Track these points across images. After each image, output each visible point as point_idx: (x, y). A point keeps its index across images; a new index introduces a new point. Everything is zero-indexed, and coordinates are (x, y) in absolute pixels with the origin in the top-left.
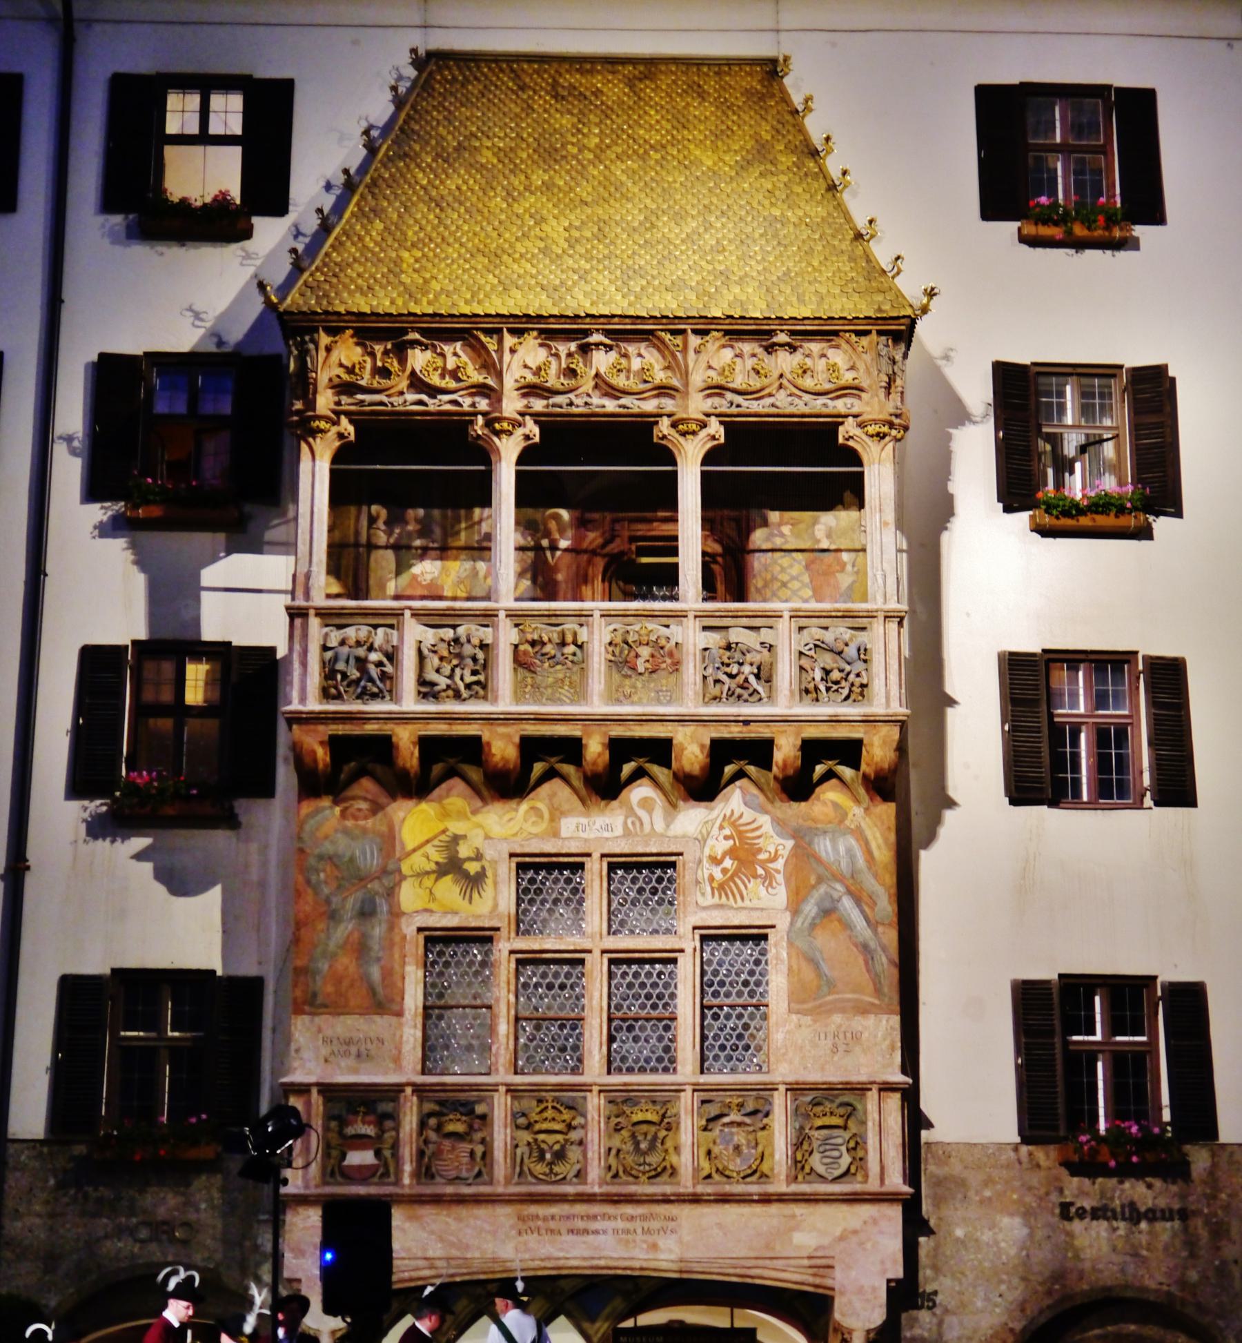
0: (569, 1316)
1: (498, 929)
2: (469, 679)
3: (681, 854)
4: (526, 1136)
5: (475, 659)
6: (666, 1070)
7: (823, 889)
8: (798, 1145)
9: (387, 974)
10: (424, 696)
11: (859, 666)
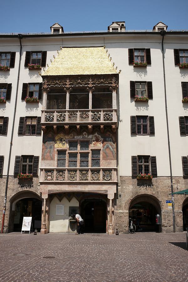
0: (75, 197)
1: (67, 150)
2: (63, 119)
3: (89, 140)
4: (70, 175)
5: (63, 116)
6: (87, 167)
7: (107, 144)
8: (103, 176)
9: (53, 155)
10: (57, 121)
11: (111, 116)
